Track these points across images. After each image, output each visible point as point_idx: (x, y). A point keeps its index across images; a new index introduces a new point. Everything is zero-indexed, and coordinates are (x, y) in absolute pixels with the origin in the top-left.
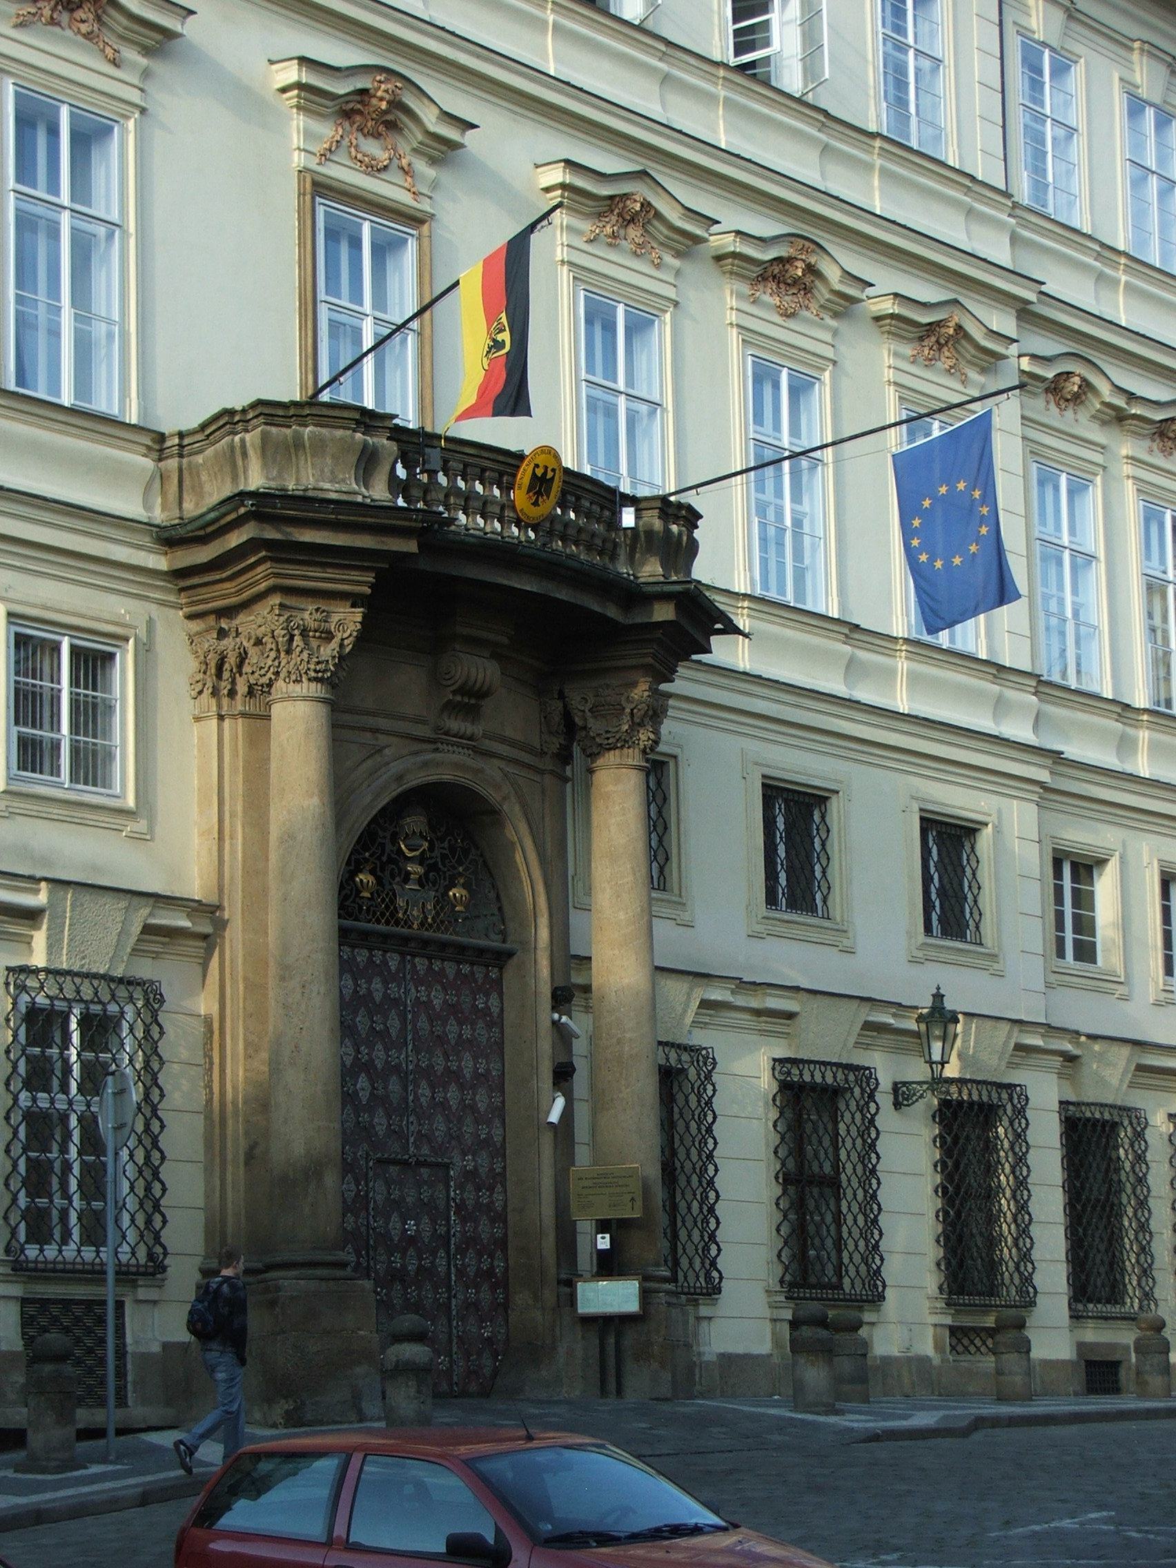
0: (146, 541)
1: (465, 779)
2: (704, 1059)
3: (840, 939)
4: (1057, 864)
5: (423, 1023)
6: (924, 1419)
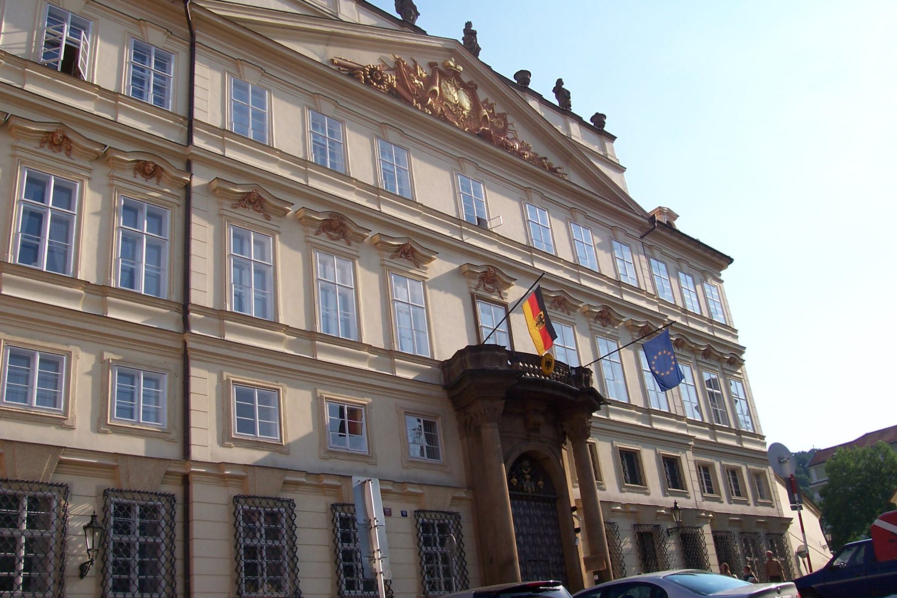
5: (536, 520)
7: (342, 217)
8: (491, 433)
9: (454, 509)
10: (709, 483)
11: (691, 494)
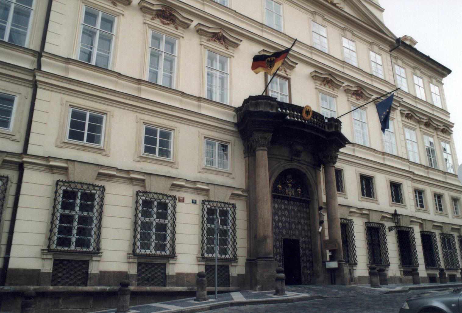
0: (233, 125)
1: (298, 168)
2: (351, 221)
3: (376, 202)
4: (415, 192)
5: (293, 213)
6: (398, 288)
7: (172, 10)
8: (262, 155)
9: (233, 202)
10: (421, 202)
11: (408, 206)
